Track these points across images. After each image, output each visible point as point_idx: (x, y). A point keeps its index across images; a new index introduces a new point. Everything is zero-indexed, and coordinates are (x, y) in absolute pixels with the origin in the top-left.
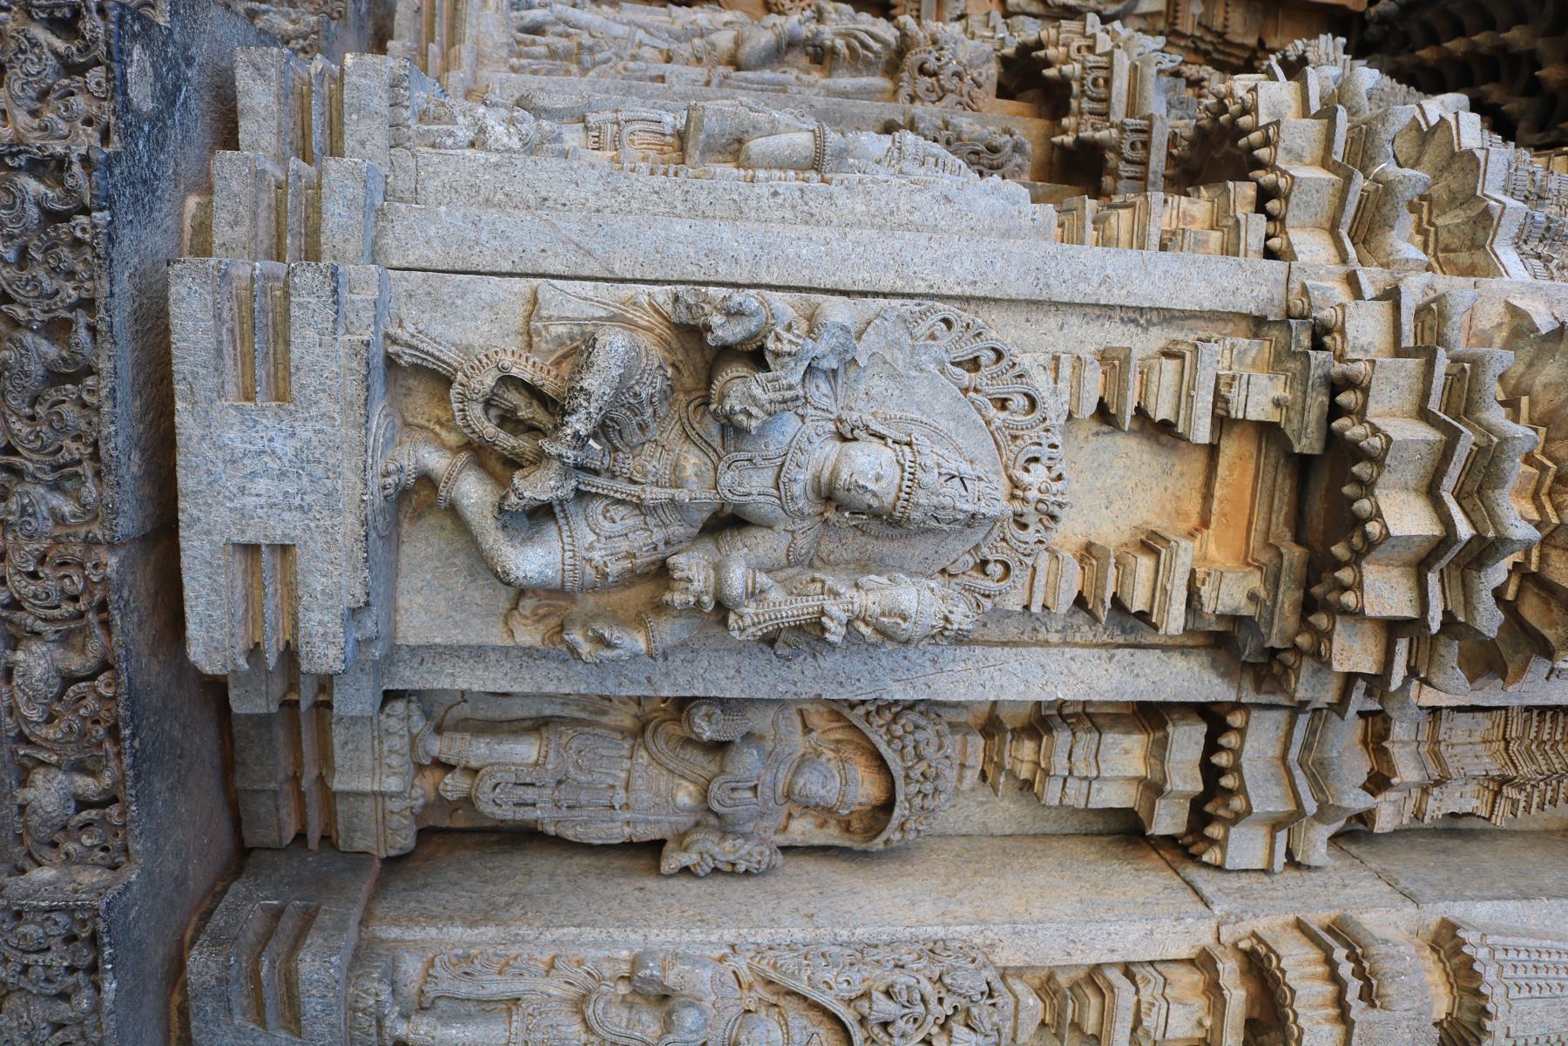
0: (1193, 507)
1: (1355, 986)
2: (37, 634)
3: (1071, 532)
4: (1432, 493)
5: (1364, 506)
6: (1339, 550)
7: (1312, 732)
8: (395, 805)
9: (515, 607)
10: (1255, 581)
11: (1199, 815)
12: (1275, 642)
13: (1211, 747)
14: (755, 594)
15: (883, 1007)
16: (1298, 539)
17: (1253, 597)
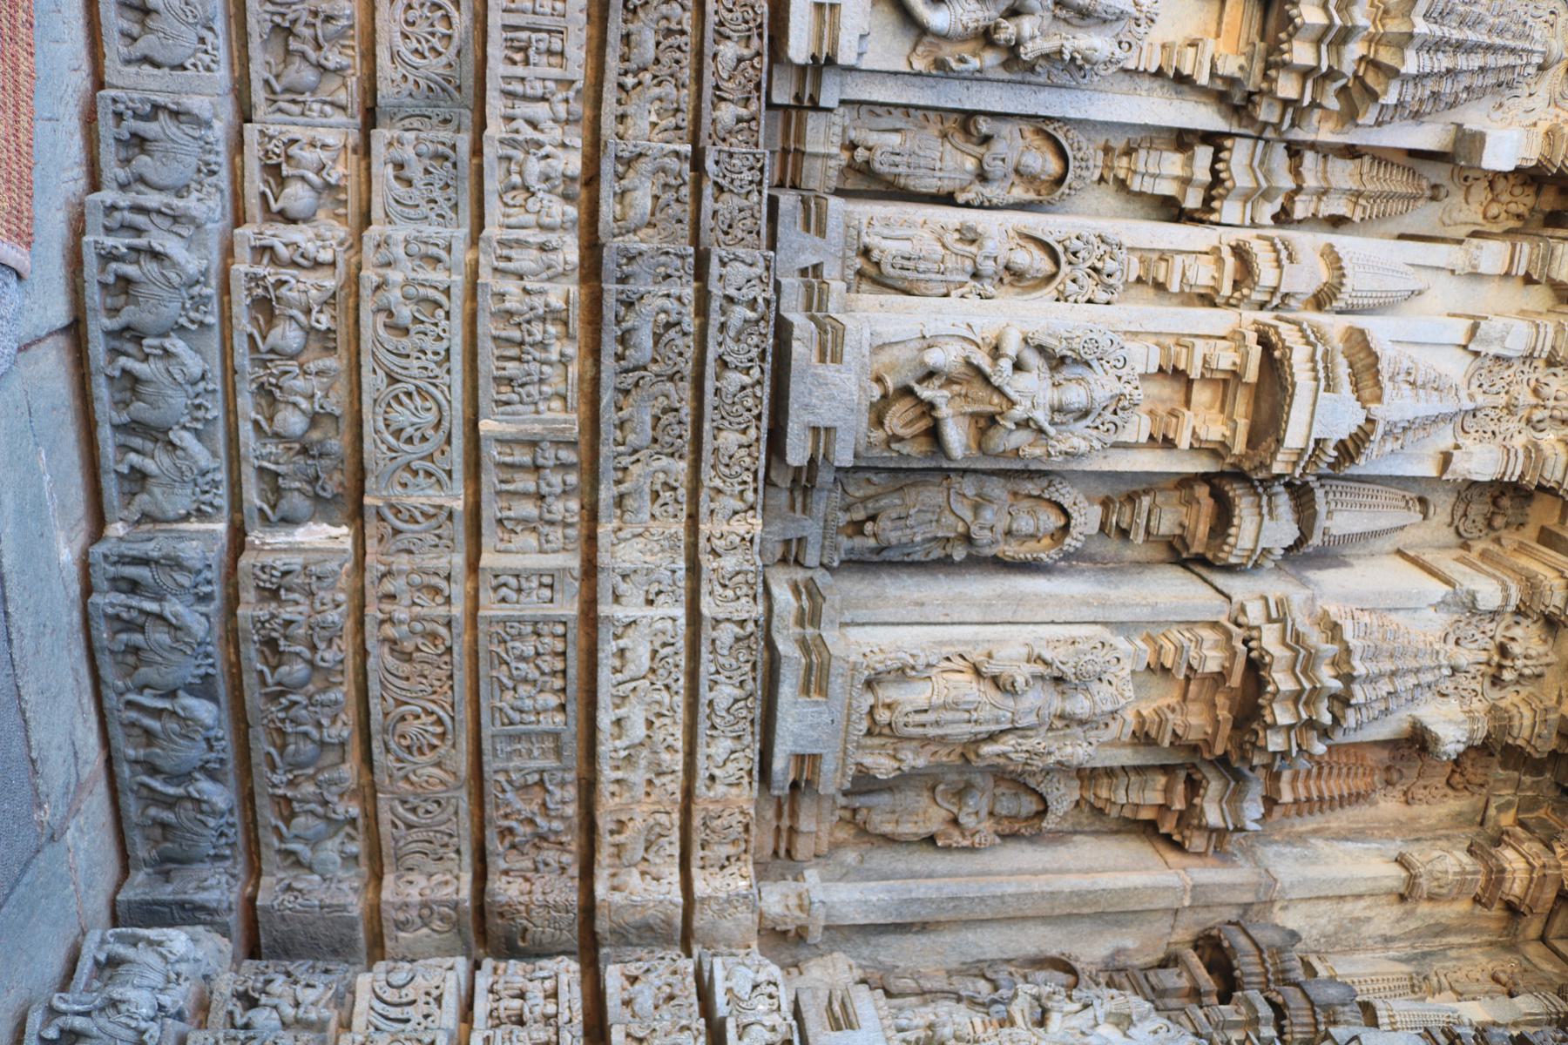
0: (1213, 28)
1: (1284, 254)
2: (728, 38)
3: (1158, 34)
4: (1325, 7)
5: (1294, 12)
6: (1283, 36)
7: (1264, 154)
8: (832, 163)
9: (914, 50)
10: (1242, 60)
11: (1208, 200)
12: (1251, 88)
13: (1216, 159)
14: (1033, 38)
15: (1077, 245)
16: (1262, 39)
17: (1241, 68)
